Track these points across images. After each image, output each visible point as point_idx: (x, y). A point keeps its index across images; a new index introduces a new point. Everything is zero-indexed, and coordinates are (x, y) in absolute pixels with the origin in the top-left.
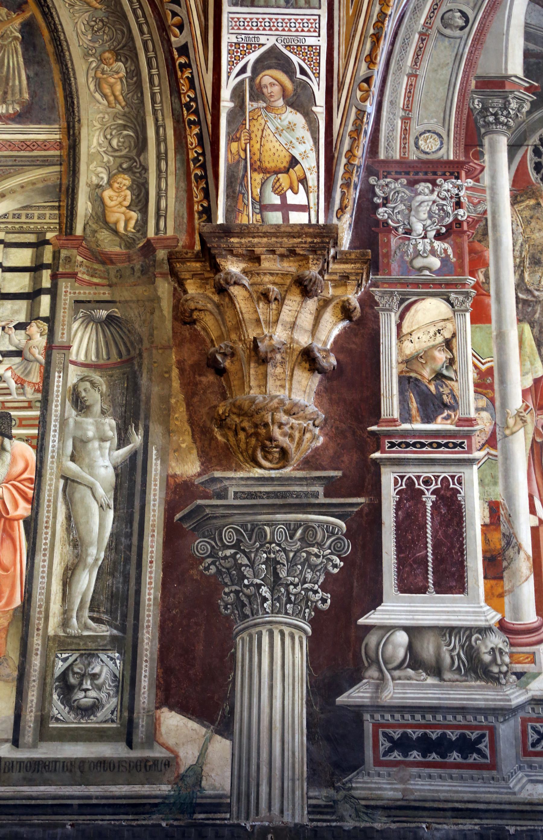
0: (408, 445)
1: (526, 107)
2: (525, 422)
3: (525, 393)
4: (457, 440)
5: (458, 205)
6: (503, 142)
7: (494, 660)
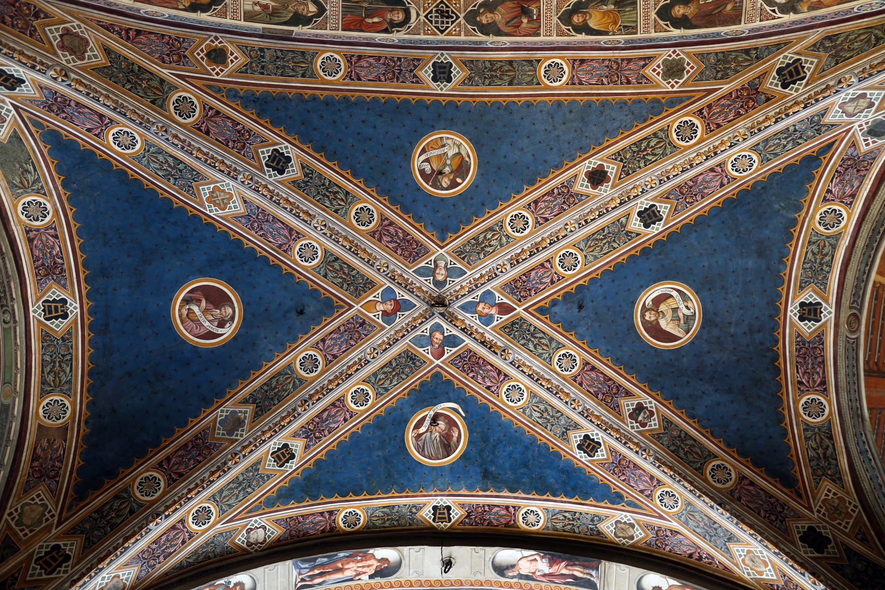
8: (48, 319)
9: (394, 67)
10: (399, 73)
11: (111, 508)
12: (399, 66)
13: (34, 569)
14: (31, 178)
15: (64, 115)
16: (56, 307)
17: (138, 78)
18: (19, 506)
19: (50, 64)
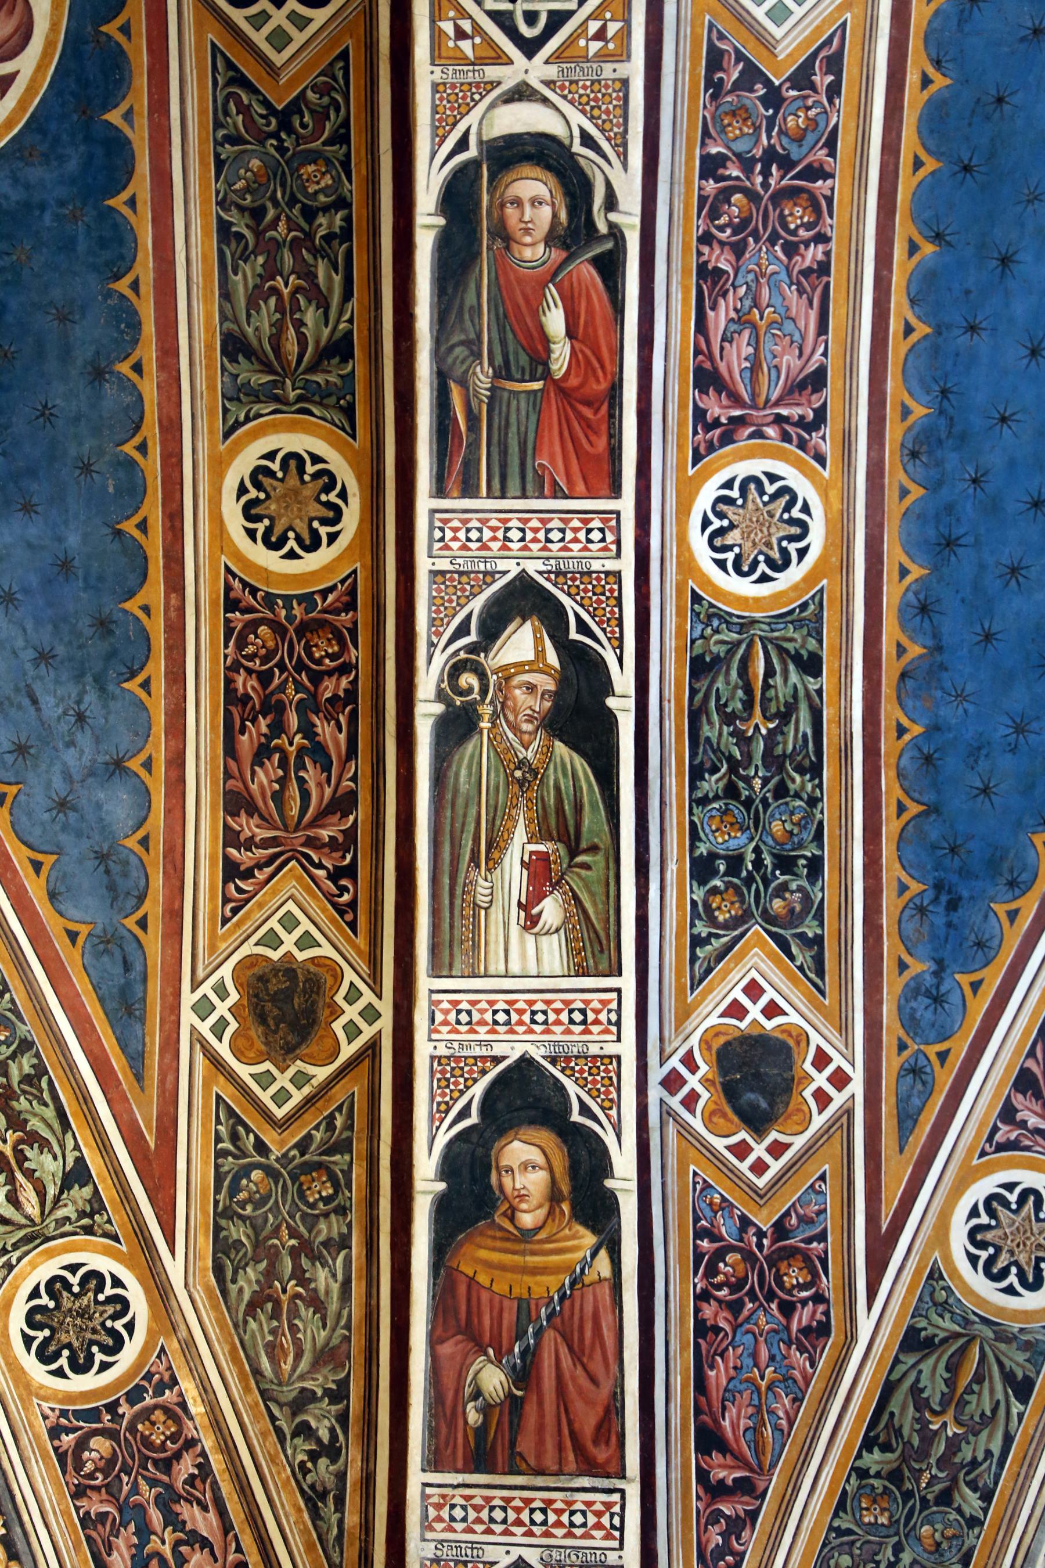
9: (752, 196)
10: (787, 164)
12: (747, 164)
17: (923, 1454)
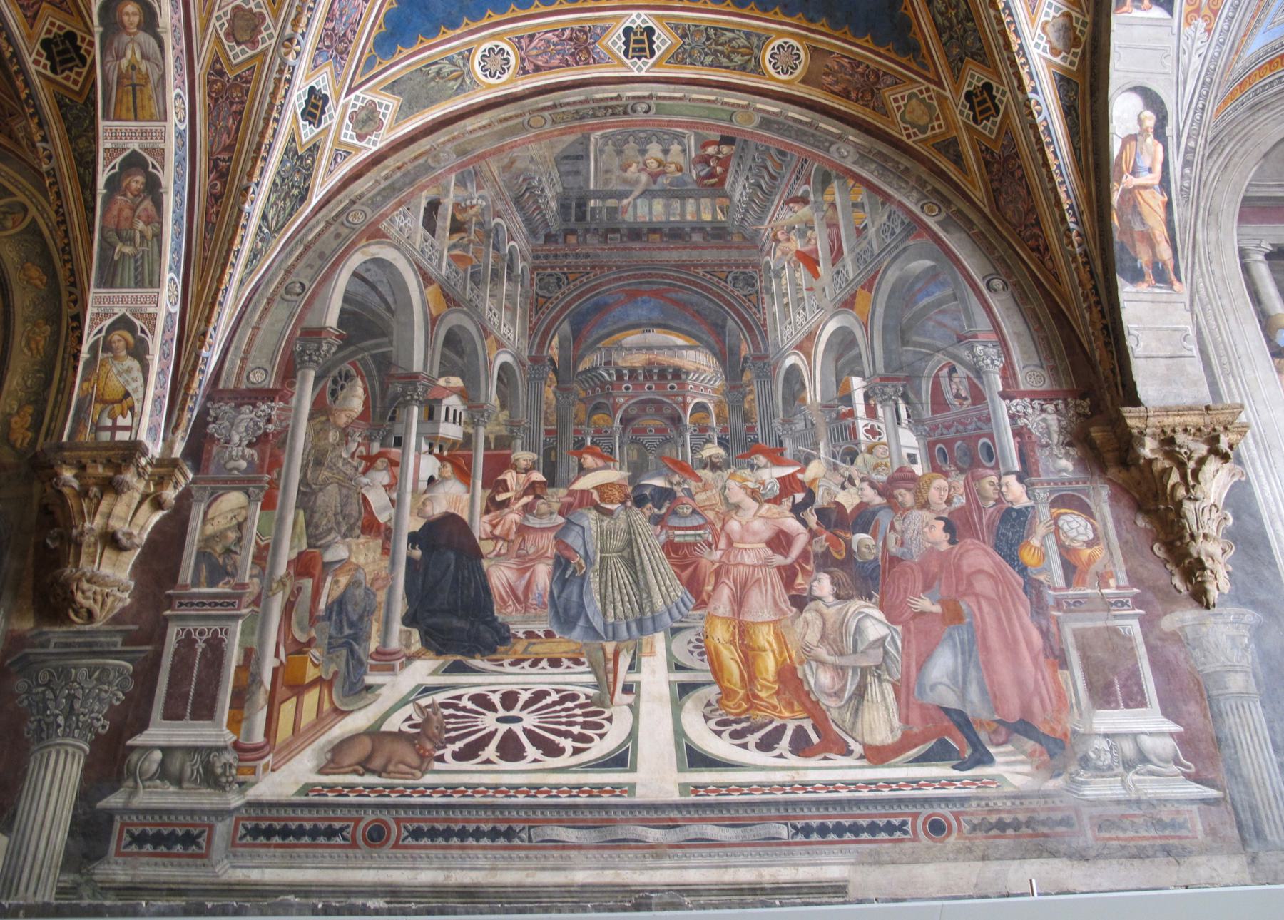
0: (193, 604)
1: (334, 349)
2: (284, 585)
3: (289, 563)
4: (229, 601)
5: (269, 421)
6: (312, 374)
7: (224, 774)
8: (652, 53)
11: (942, 14)
13: (985, 127)
14: (447, 68)
15: (349, 34)
16: (636, 42)
18: (902, 125)
19: (279, 61)
